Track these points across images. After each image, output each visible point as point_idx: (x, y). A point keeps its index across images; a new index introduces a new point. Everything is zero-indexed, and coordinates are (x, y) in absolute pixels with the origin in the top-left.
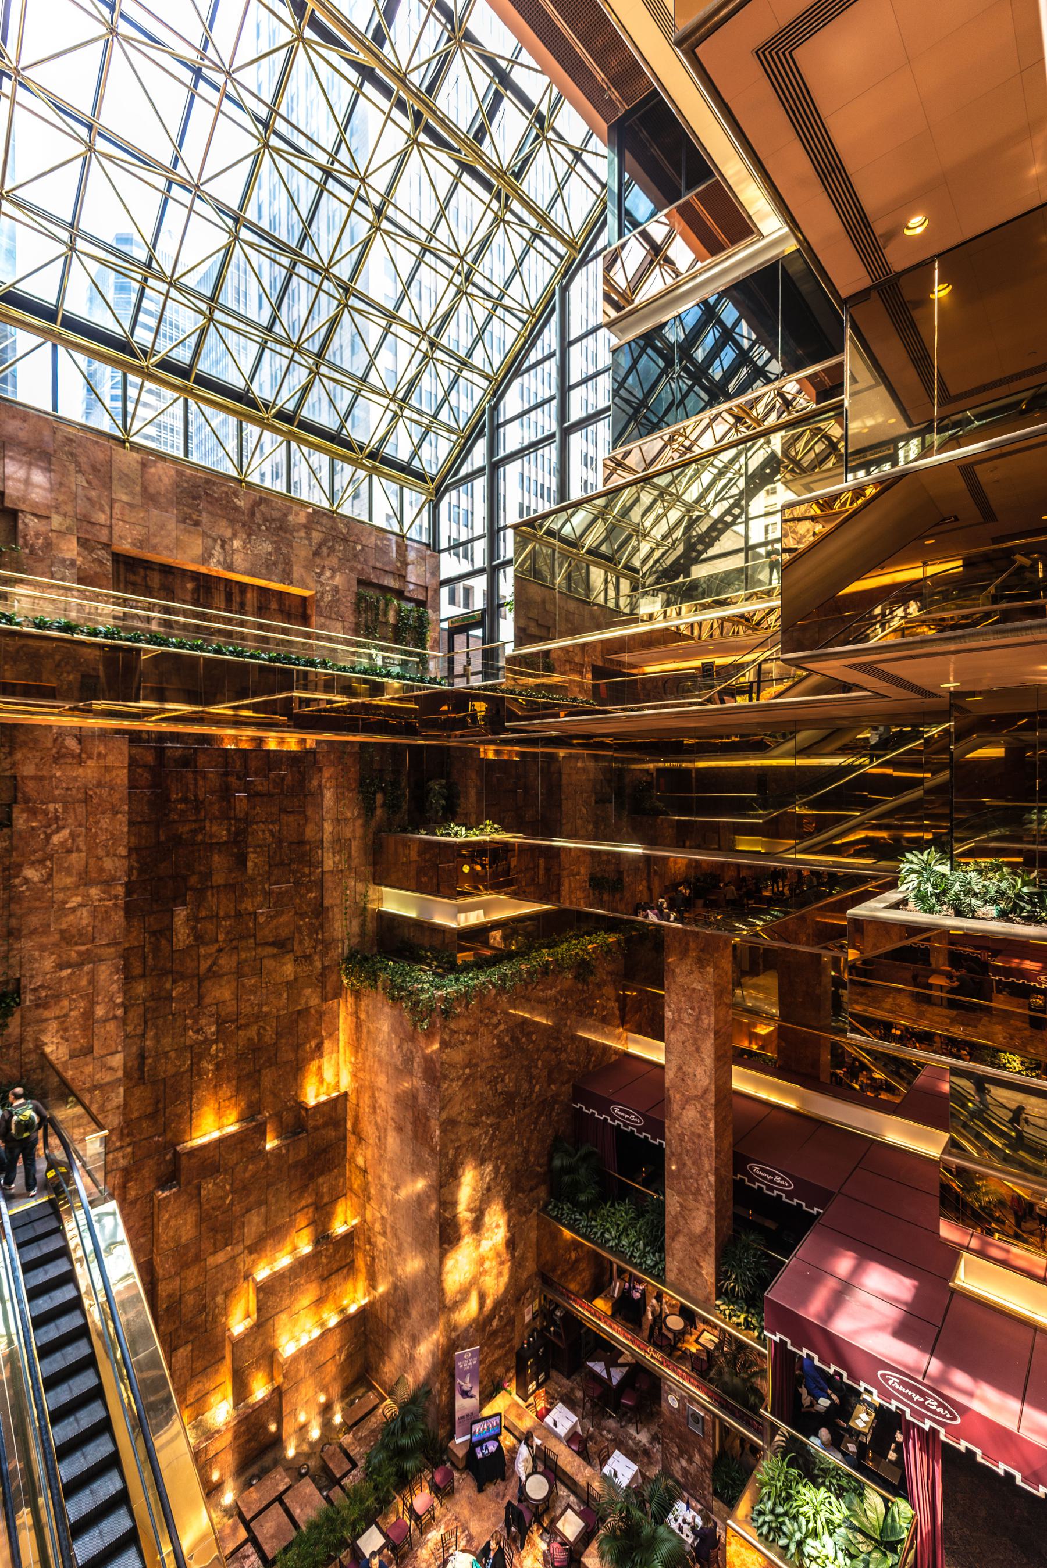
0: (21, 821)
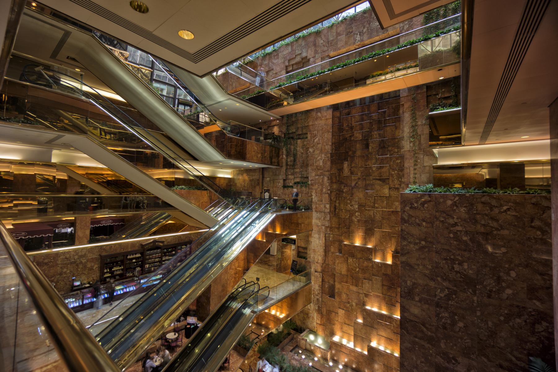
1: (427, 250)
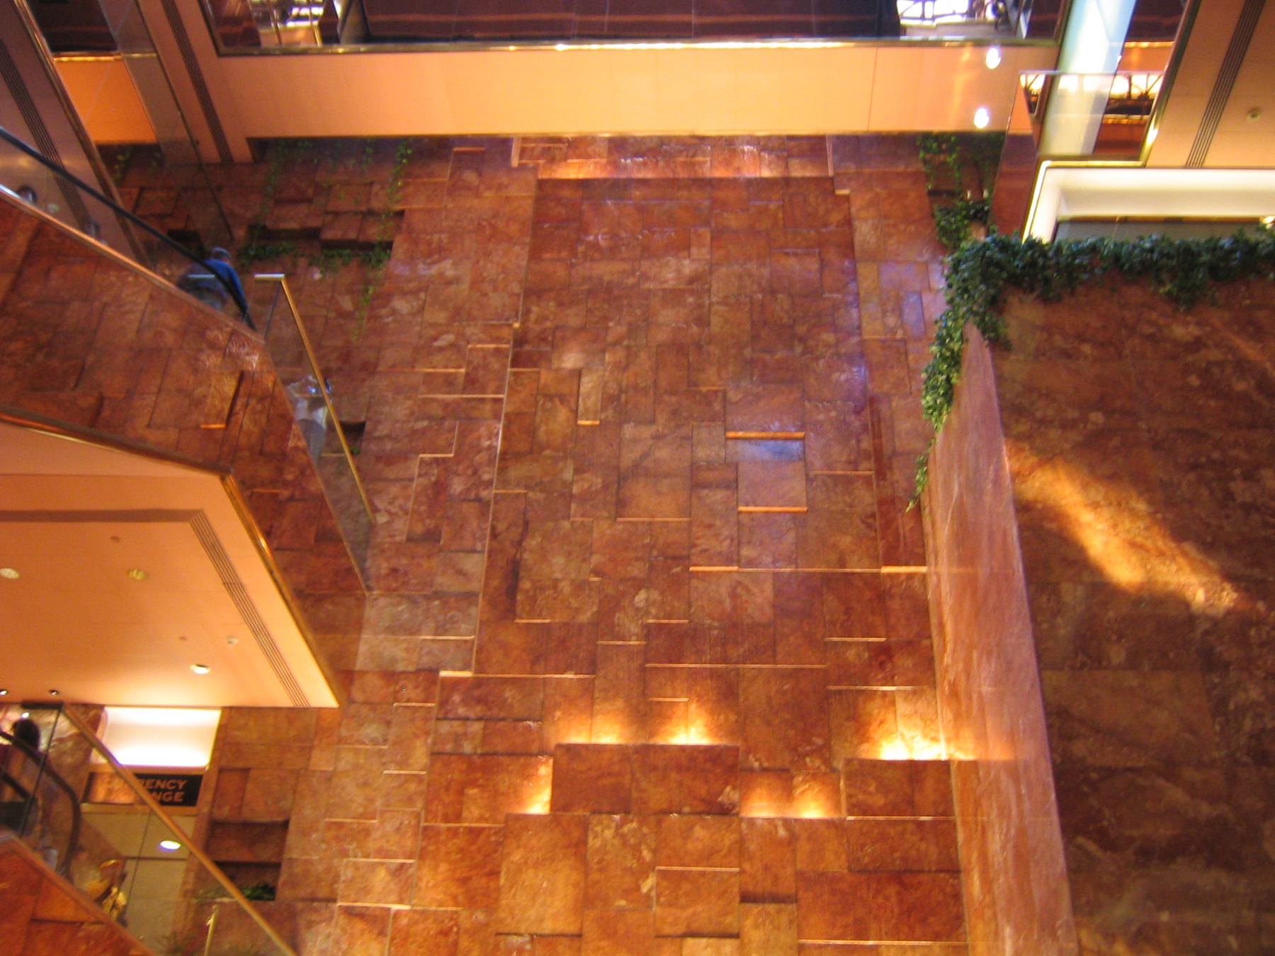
0: (400, 250)
1: (1116, 441)
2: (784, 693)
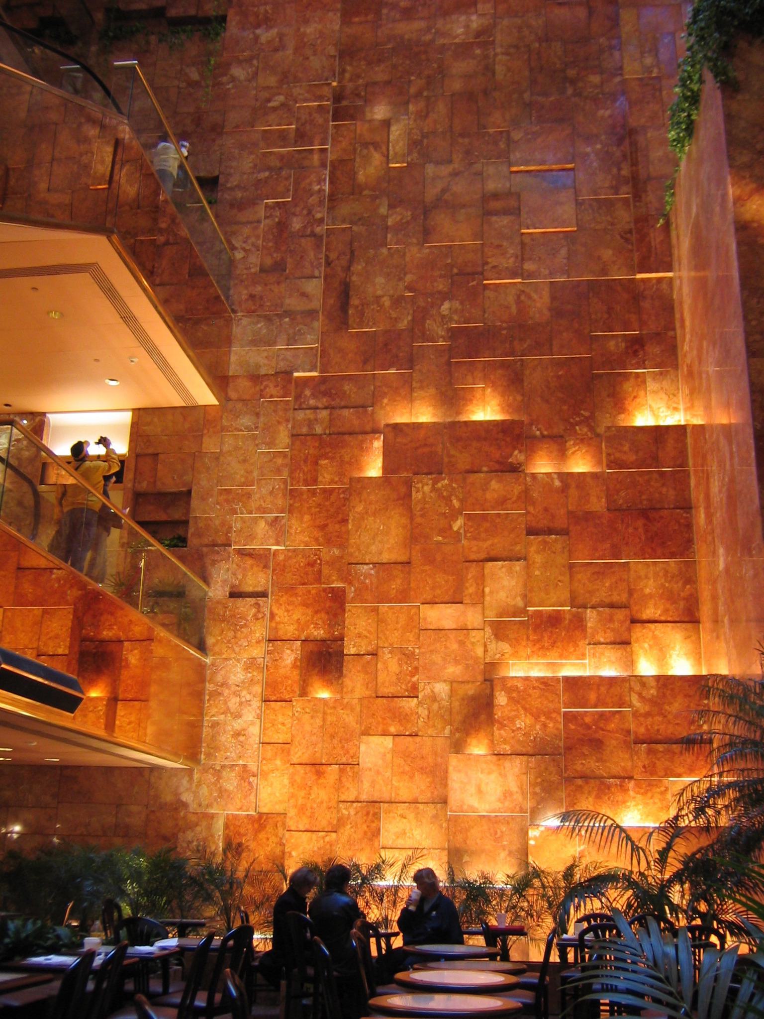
0: (234, 23)
2: (559, 377)
